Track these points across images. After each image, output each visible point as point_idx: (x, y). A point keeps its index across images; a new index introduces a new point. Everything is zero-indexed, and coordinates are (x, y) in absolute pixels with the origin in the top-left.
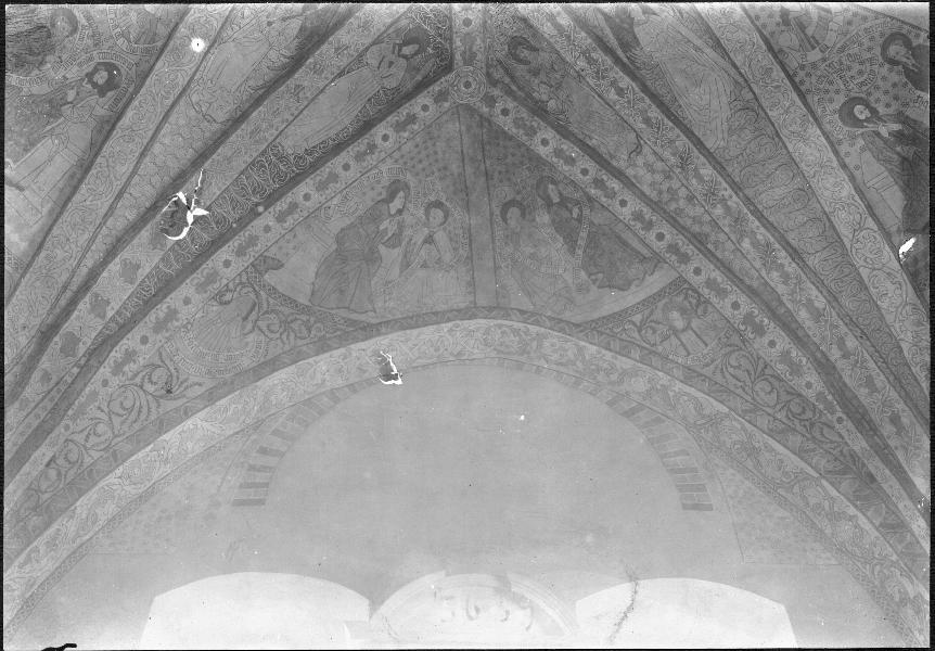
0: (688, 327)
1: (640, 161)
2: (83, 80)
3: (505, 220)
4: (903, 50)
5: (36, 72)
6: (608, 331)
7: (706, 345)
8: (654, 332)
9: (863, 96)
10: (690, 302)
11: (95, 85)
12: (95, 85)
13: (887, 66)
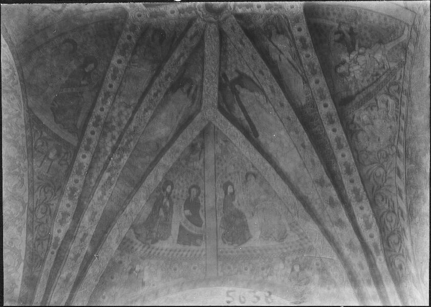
0: (52, 160)
1: (122, 108)
3: (64, 43)
4: (195, 194)
6: (32, 124)
7: (47, 173)
8: (42, 145)
10: (64, 156)
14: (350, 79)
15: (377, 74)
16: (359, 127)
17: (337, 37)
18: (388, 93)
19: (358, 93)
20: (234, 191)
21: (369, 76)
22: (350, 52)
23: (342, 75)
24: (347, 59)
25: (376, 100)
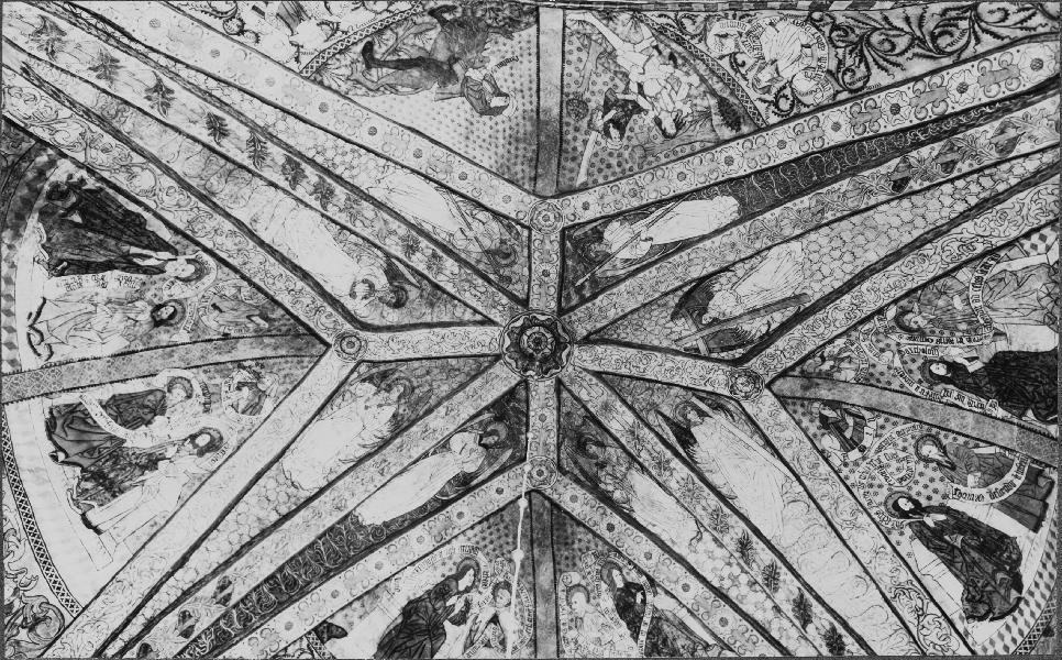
2: (186, 440)
5: (144, 426)
9: (905, 489)
11: (195, 446)
12: (195, 446)
13: (922, 464)
14: (687, 109)
15: (672, 57)
16: (784, 87)
17: (614, 132)
18: (703, 37)
19: (713, 93)
20: (944, 362)
21: (678, 73)
22: (638, 109)
23: (679, 125)
24: (652, 114)
25: (722, 57)
